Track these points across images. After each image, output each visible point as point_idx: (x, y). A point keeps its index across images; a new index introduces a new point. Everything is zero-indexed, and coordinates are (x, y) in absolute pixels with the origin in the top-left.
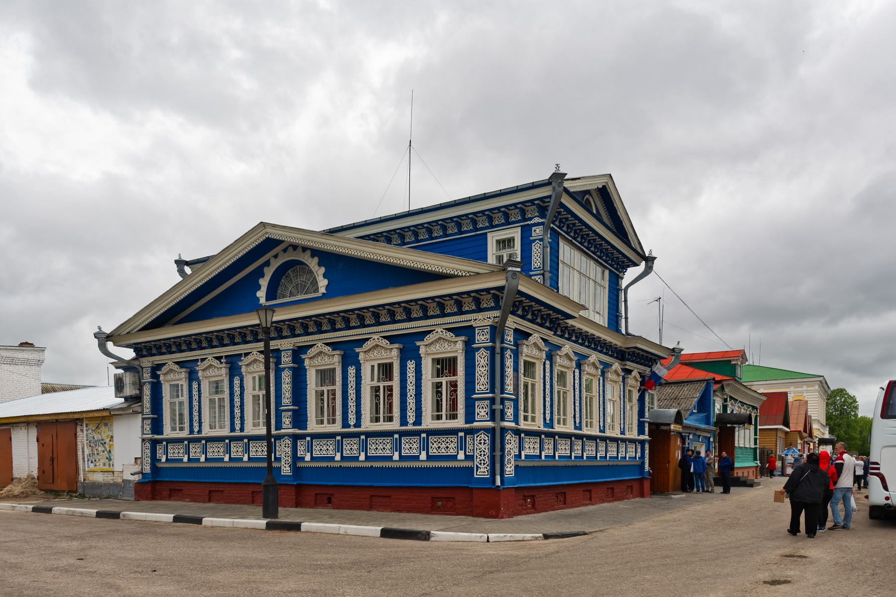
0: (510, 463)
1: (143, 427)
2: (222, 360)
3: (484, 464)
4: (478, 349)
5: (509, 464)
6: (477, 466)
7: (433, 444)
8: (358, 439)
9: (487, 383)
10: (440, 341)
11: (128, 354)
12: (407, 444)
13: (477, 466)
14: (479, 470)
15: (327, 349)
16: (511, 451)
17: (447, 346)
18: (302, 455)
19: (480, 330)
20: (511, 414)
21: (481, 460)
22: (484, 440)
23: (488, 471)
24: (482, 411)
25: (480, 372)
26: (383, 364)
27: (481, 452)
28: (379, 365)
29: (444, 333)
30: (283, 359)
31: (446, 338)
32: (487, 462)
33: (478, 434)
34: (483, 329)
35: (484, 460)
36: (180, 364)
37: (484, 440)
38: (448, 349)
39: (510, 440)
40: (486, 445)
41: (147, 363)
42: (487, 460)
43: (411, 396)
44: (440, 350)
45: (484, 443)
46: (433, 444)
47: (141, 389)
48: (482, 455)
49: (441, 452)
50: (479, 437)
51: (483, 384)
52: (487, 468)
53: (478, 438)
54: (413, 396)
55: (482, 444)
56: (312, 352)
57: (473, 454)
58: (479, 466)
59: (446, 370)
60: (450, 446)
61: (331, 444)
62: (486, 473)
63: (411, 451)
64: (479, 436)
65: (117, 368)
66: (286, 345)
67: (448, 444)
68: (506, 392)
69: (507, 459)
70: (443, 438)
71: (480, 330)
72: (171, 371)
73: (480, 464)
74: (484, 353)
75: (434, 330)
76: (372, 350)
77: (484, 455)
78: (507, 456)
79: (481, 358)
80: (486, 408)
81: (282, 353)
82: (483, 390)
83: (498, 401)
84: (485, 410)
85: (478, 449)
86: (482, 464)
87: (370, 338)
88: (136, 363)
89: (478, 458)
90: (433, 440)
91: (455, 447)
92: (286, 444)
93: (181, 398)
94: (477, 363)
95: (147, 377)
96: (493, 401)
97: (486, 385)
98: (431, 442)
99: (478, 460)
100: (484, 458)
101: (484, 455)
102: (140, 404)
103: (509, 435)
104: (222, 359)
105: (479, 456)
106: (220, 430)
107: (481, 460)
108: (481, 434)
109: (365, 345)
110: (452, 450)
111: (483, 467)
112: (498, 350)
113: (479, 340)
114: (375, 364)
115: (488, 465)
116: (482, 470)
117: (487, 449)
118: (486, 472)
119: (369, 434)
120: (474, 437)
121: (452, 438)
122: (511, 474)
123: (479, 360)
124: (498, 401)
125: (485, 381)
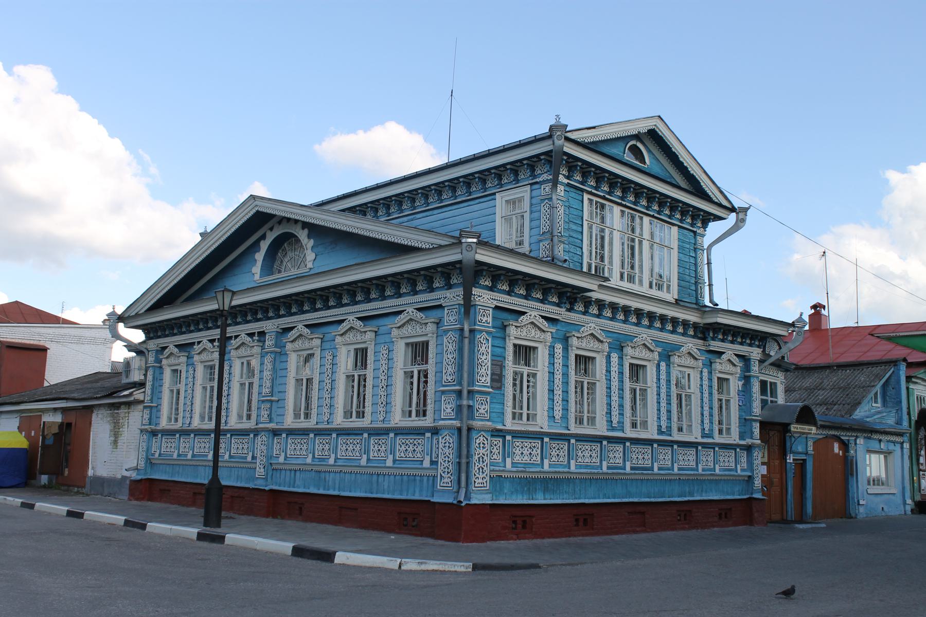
0: (483, 472)
1: (142, 417)
2: (215, 344)
5: (481, 474)
6: (441, 475)
7: (401, 446)
8: (330, 438)
9: (454, 373)
10: (412, 323)
11: (137, 336)
12: (376, 446)
13: (441, 475)
14: (443, 481)
15: (307, 331)
16: (485, 457)
17: (418, 329)
18: (278, 454)
19: (449, 309)
20: (487, 412)
22: (449, 443)
23: (451, 481)
24: (448, 408)
25: (447, 360)
26: (360, 349)
27: (445, 457)
28: (356, 350)
29: (414, 313)
30: (267, 343)
31: (416, 319)
36: (180, 347)
37: (449, 443)
38: (420, 332)
40: (451, 449)
41: (153, 345)
42: (451, 468)
43: (383, 387)
44: (412, 333)
45: (449, 447)
46: (401, 446)
47: (145, 375)
48: (447, 462)
50: (444, 439)
51: (450, 375)
52: (450, 478)
54: (385, 387)
55: (447, 448)
56: (293, 334)
57: (437, 460)
58: (443, 475)
59: (419, 357)
61: (305, 443)
63: (379, 455)
64: (443, 438)
65: (129, 351)
66: (270, 326)
67: (416, 446)
68: (477, 383)
69: (476, 468)
71: (449, 309)
72: (171, 354)
73: (444, 472)
74: (452, 337)
75: (405, 310)
76: (348, 333)
78: (477, 464)
79: (450, 343)
80: (452, 404)
81: (267, 336)
82: (449, 382)
83: (465, 393)
87: (345, 320)
88: (145, 346)
89: (442, 465)
90: (401, 441)
91: (422, 451)
93: (178, 385)
95: (151, 359)
96: (459, 393)
97: (453, 375)
98: (399, 444)
99: (442, 467)
102: (143, 390)
103: (482, 438)
104: (215, 342)
105: (443, 463)
106: (208, 422)
108: (446, 435)
109: (341, 327)
111: (447, 476)
112: (467, 333)
113: (448, 321)
114: (352, 347)
115: (451, 475)
116: (446, 480)
117: (451, 454)
120: (438, 439)
121: (419, 439)
122: (484, 487)
124: (465, 393)
125: (452, 372)
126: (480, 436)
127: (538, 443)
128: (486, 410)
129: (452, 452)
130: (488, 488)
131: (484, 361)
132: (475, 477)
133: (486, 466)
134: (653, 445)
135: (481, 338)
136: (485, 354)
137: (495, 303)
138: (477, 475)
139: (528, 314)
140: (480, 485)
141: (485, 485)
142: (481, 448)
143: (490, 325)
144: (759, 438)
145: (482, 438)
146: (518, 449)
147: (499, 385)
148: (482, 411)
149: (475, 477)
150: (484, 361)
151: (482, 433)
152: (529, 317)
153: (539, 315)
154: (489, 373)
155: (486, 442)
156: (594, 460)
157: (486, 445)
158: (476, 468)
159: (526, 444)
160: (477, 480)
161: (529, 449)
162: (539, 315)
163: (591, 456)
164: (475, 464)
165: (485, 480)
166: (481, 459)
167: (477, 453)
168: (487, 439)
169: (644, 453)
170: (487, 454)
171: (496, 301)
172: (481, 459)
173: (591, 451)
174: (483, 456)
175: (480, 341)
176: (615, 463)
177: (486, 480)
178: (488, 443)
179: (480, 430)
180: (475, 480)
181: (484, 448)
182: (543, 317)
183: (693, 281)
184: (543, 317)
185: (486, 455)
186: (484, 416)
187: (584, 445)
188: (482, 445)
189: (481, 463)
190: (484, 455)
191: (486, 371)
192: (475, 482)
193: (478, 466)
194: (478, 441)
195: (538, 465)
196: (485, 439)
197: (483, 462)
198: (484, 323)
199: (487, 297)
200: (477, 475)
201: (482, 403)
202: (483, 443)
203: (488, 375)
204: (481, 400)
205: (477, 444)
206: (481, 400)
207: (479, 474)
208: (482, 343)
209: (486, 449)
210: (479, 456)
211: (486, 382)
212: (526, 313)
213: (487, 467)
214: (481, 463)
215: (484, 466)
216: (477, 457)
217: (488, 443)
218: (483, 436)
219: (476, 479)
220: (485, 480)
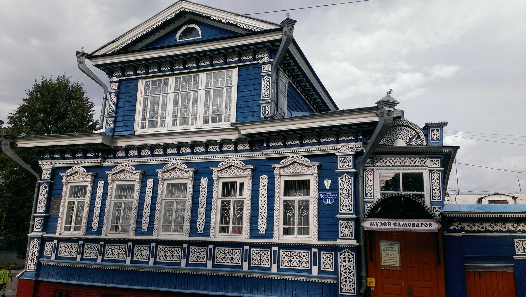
3: (350, 282)
4: (341, 174)
33: (341, 253)
39: (350, 258)
60: (263, 259)
69: (343, 277)
70: (295, 252)
78: (343, 274)
84: (349, 229)
92: (345, 258)
94: (340, 187)
107: (346, 278)
110: (265, 263)
126: (345, 252)
128: (351, 232)
130: (355, 294)
133: (352, 276)
135: (342, 178)
138: (345, 283)
140: (348, 291)
141: (353, 291)
142: (347, 262)
143: (352, 168)
145: (347, 254)
148: (346, 232)
154: (352, 203)
155: (351, 257)
157: (352, 259)
160: (344, 287)
164: (341, 274)
165: (352, 288)
167: (342, 265)
168: (353, 255)
170: (353, 266)
175: (342, 181)
177: (353, 287)
180: (342, 287)
181: (349, 261)
185: (352, 267)
188: (347, 259)
189: (347, 273)
190: (350, 267)
191: (350, 201)
192: (342, 289)
193: (344, 275)
194: (342, 256)
196: (349, 254)
197: (349, 273)
198: (345, 167)
201: (346, 226)
203: (351, 205)
204: (345, 224)
205: (341, 259)
206: (345, 224)
208: (344, 182)
209: (353, 262)
213: (354, 277)
214: (347, 273)
215: (351, 276)
217: (353, 258)
219: (343, 286)
220: (352, 288)
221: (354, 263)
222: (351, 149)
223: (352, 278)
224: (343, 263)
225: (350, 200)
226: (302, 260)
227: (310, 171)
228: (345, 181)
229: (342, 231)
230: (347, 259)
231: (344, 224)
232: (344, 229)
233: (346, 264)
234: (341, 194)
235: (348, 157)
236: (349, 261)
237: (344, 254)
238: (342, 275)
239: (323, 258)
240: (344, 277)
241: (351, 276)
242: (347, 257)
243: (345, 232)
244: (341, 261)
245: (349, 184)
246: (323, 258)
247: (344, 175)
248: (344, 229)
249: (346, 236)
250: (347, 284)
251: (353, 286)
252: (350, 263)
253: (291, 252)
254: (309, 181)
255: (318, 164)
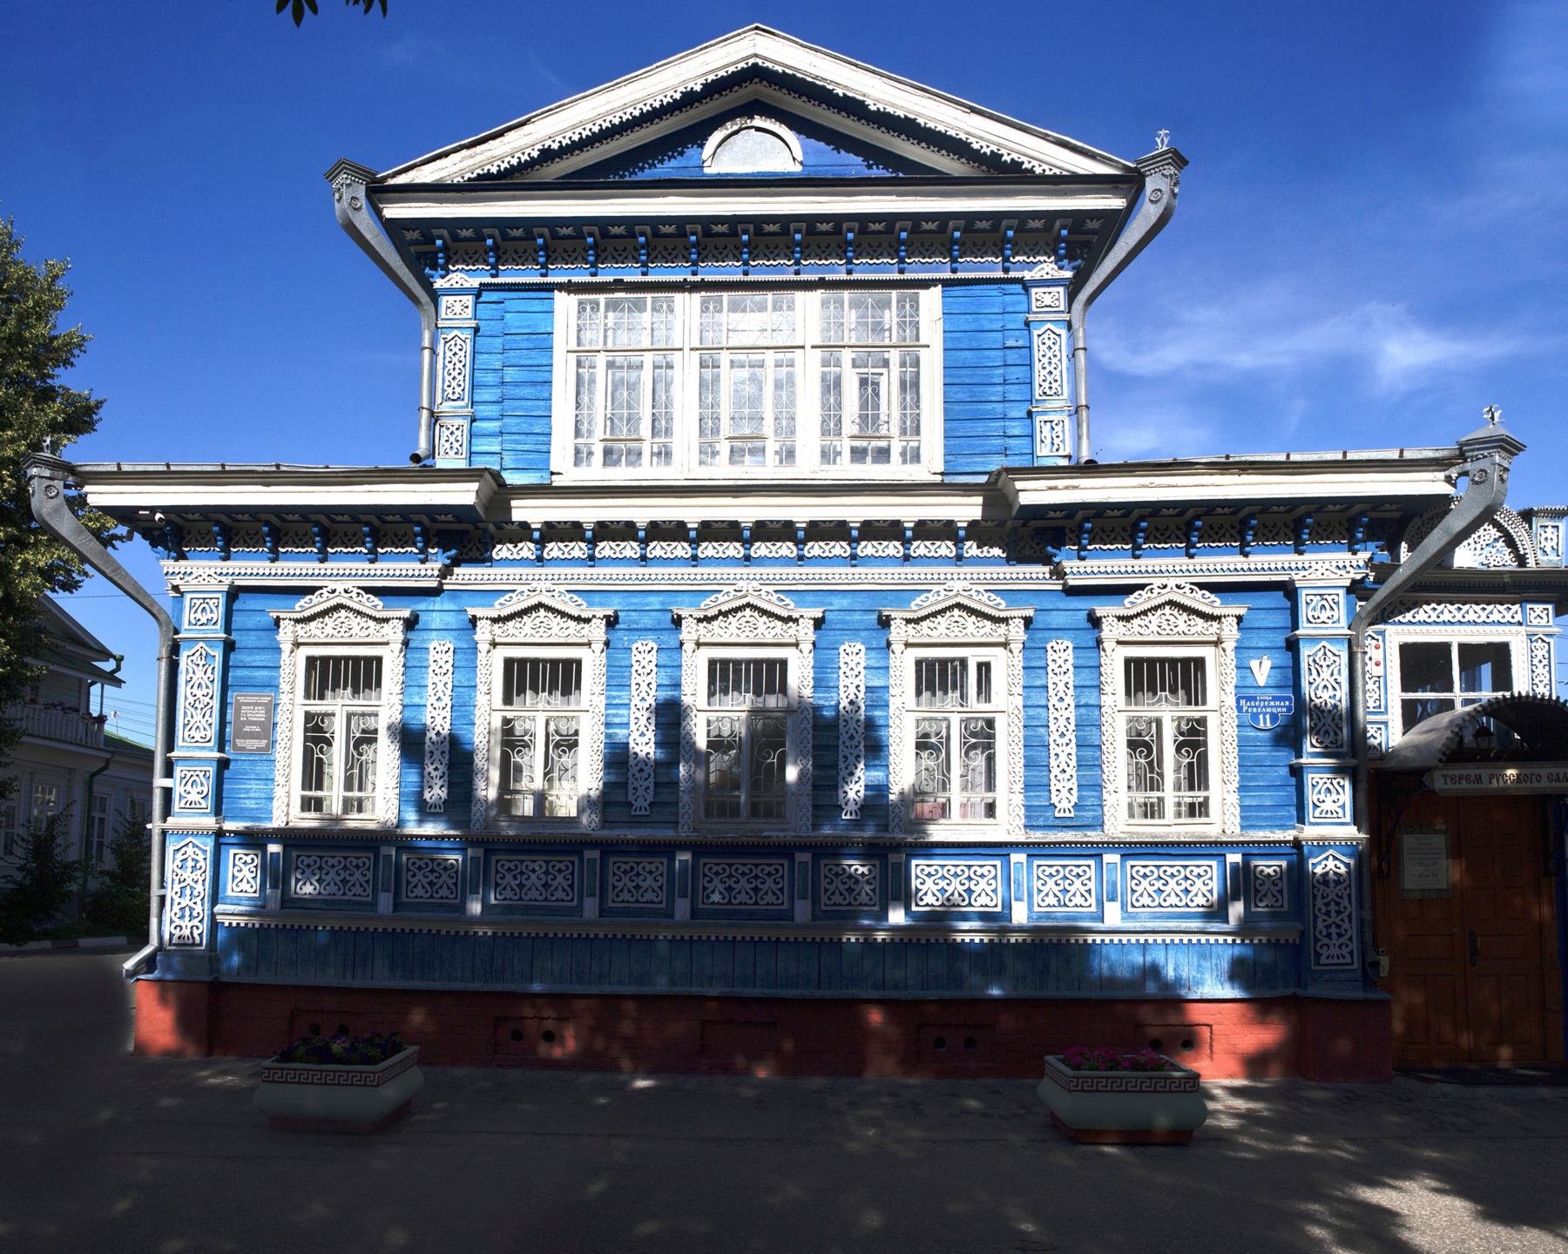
21: (1328, 927)
32: (1346, 931)
34: (205, 599)
35: (1338, 926)
49: (553, 898)
53: (179, 856)
62: (1348, 960)
77: (1339, 913)
78: (177, 900)
85: (177, 881)
86: (1334, 936)
100: (1338, 921)
101: (1339, 913)
103: (190, 850)
118: (1347, 956)
119: (1133, 850)
123: (191, 671)
127: (366, 858)
129: (201, 879)
131: (202, 698)
132: (174, 925)
134: (793, 855)
136: (204, 686)
137: (227, 581)
139: (324, 590)
144: (1348, 819)
146: (533, 876)
147: (263, 743)
148: (194, 797)
149: (174, 925)
150: (202, 698)
151: (190, 839)
152: (326, 594)
153: (359, 588)
156: (560, 894)
157: (202, 863)
158: (176, 909)
159: (331, 862)
161: (341, 872)
162: (359, 588)
163: (546, 885)
166: (188, 892)
169: (756, 877)
170: (204, 880)
171: (230, 578)
172: (188, 892)
173: (547, 873)
174: (192, 884)
176: (637, 901)
178: (205, 859)
179: (184, 832)
182: (368, 590)
183: (1019, 411)
184: (368, 590)
186: (198, 806)
187: (522, 862)
188: (190, 863)
195: (366, 904)
196: (196, 849)
199: (208, 572)
200: (178, 922)
202: (193, 860)
207: (182, 917)
210: (183, 885)
211: (208, 739)
212: (321, 588)
213: (203, 905)
215: (195, 903)
216: (177, 888)
217: (205, 859)
218: (195, 846)
219: (175, 928)
221: (205, 872)
222: (220, 578)
223: (198, 908)
224: (180, 872)
225: (208, 714)
226: (555, 883)
227: (383, 631)
228: (199, 662)
229: (184, 794)
230: (190, 863)
231: (189, 775)
232: (188, 788)
233: (185, 876)
234: (186, 698)
235: (211, 599)
236: (194, 868)
237: (183, 851)
238: (176, 903)
239: (497, 872)
240: (179, 907)
241: (195, 903)
242: (190, 859)
243: (190, 797)
244: (176, 869)
245: (209, 671)
246: (497, 872)
247: (198, 647)
248: (188, 788)
249: (193, 806)
250: (183, 925)
251: (198, 928)
252: (195, 873)
253: (730, 865)
254: (379, 660)
255: (406, 614)
